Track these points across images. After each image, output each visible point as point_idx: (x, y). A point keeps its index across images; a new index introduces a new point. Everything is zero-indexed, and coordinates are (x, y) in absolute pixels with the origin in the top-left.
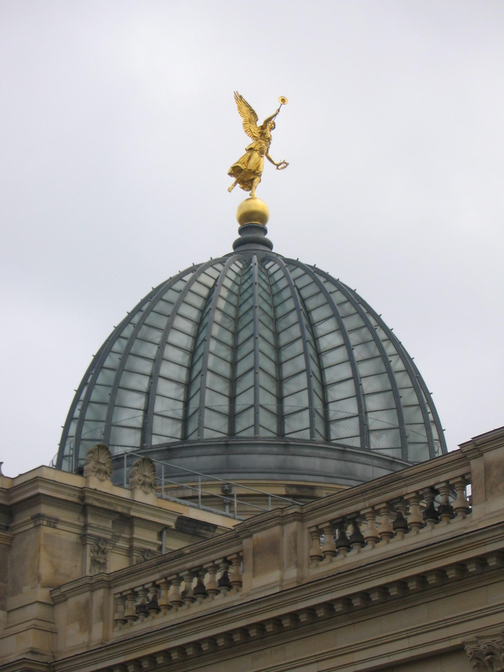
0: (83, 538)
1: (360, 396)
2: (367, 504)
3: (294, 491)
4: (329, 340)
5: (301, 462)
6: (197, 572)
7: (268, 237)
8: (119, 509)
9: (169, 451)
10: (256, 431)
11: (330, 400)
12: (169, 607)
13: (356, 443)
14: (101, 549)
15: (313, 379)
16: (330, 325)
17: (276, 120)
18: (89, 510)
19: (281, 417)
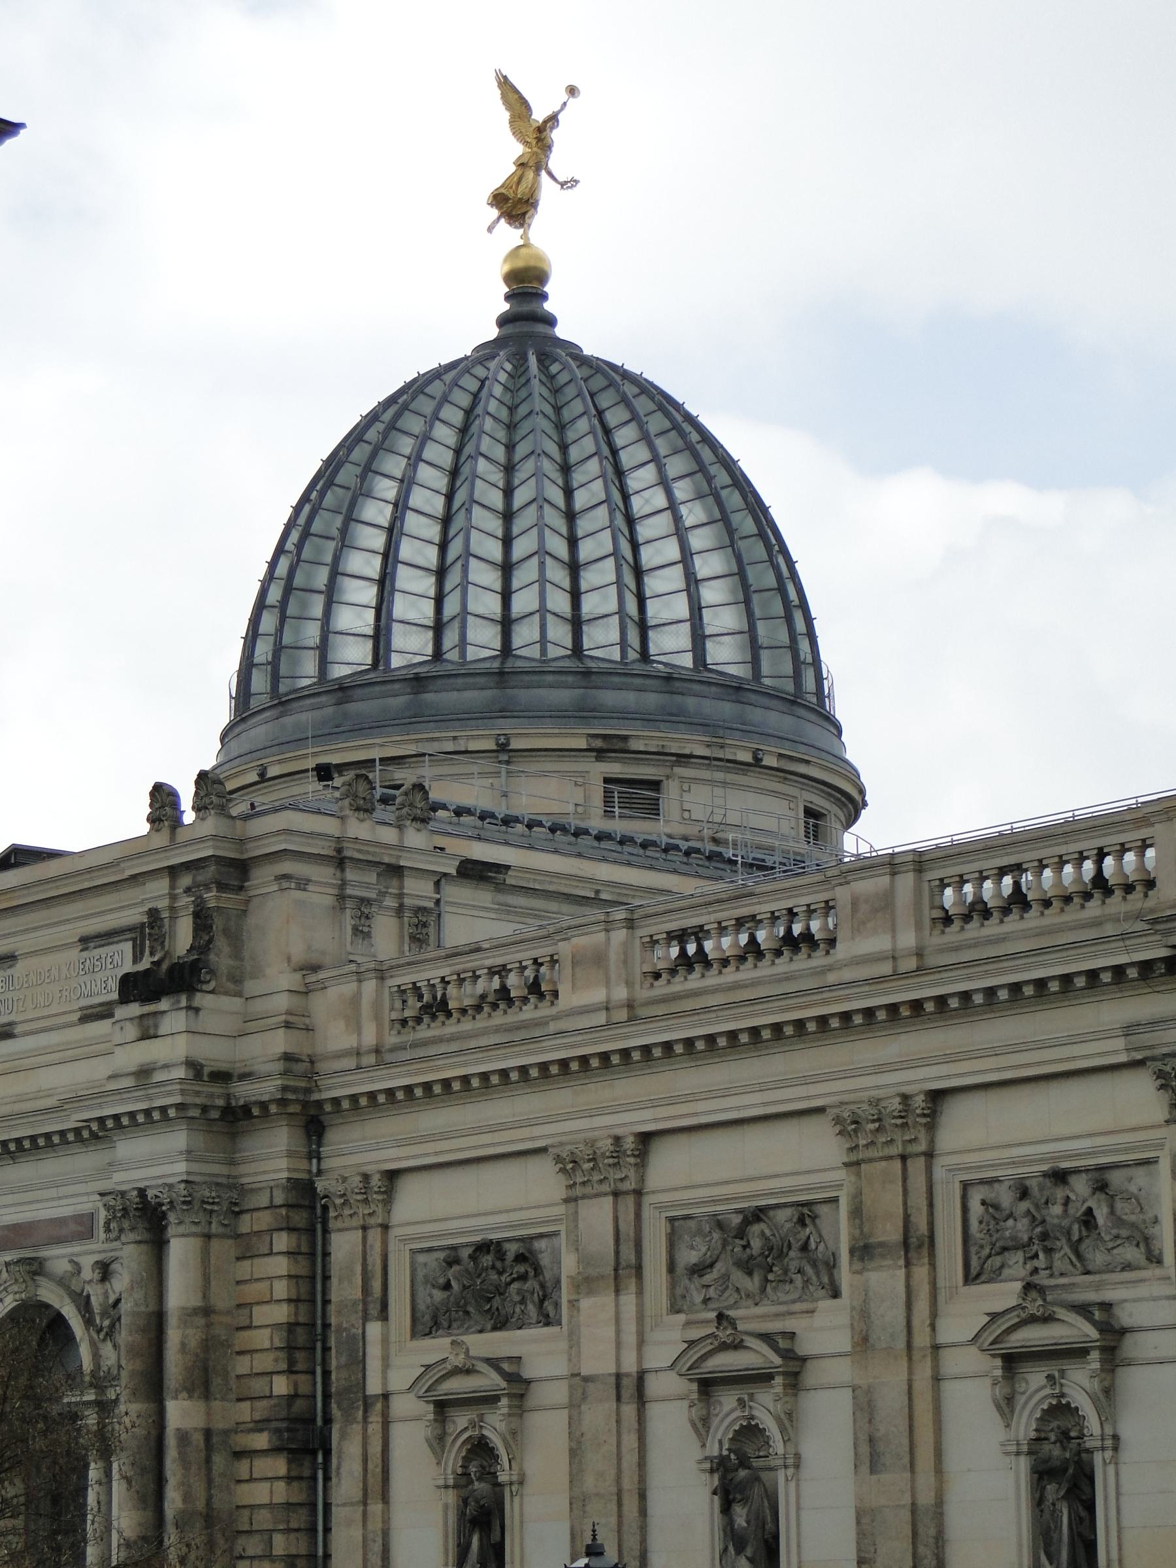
0: (342, 897)
1: (692, 583)
2: (713, 917)
3: (598, 743)
4: (648, 500)
5: (609, 698)
6: (501, 971)
7: (548, 306)
8: (386, 860)
9: (417, 681)
10: (544, 651)
11: (648, 594)
13: (687, 661)
15: (625, 567)
16: (648, 474)
17: (560, 117)
18: (348, 864)
19: (577, 623)
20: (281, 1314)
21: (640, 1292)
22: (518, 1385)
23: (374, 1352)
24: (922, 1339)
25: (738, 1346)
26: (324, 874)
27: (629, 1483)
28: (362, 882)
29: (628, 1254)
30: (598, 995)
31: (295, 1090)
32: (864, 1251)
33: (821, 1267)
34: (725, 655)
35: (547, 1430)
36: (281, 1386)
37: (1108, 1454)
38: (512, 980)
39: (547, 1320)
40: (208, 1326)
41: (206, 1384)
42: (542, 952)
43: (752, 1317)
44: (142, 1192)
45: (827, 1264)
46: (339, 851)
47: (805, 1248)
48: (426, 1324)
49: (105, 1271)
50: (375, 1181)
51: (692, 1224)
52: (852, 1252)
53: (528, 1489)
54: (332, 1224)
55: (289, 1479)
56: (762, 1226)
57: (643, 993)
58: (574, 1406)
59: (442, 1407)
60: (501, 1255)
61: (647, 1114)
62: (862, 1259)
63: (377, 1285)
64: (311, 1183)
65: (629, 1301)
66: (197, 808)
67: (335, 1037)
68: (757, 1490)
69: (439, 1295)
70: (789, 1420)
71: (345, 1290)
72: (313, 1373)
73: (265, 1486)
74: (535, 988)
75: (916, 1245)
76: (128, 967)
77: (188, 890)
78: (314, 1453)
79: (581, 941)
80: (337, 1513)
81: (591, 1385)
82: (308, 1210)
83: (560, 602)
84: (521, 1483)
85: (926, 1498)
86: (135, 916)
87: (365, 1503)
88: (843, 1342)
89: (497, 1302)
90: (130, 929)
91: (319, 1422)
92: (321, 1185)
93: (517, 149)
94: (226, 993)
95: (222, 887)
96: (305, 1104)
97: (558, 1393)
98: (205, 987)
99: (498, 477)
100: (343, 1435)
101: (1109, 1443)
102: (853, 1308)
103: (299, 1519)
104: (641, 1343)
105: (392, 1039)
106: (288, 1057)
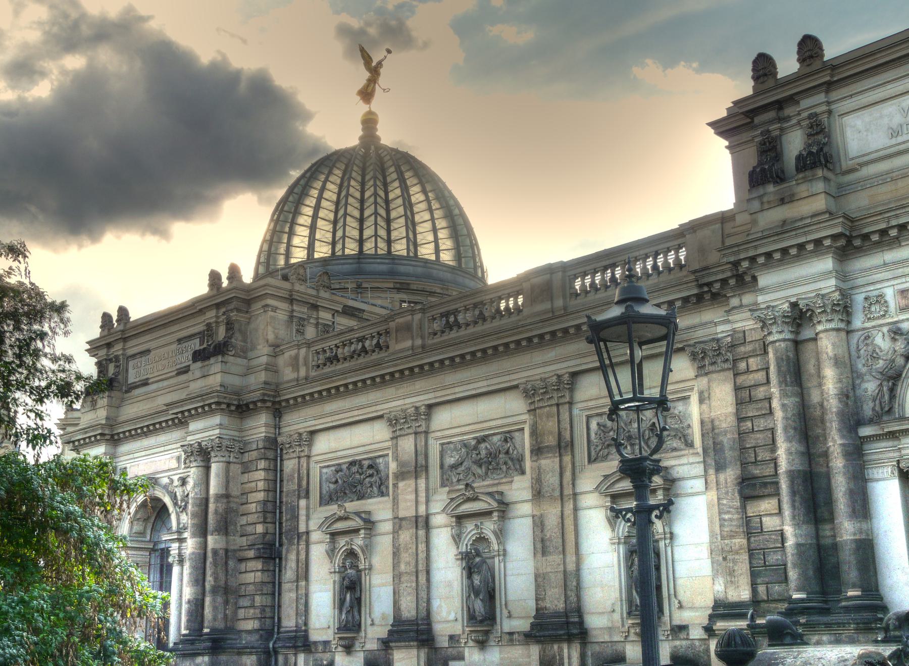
0: (291, 317)
1: (435, 230)
3: (398, 286)
6: (361, 339)
10: (376, 251)
12: (345, 359)
13: (433, 258)
14: (301, 324)
18: (295, 302)
19: (389, 242)
20: (261, 496)
21: (427, 478)
22: (370, 524)
23: (303, 512)
24: (568, 491)
25: (475, 499)
26: (284, 306)
27: (421, 567)
28: (301, 311)
29: (421, 460)
30: (408, 343)
31: (269, 396)
32: (538, 451)
33: (516, 462)
34: (447, 257)
35: (384, 544)
36: (260, 529)
37: (668, 541)
38: (367, 344)
39: (382, 494)
40: (228, 502)
41: (226, 529)
42: (381, 328)
43: (479, 485)
44: (200, 444)
45: (518, 460)
46: (291, 296)
47: (507, 453)
48: (327, 499)
49: (184, 482)
50: (304, 436)
51: (452, 446)
52: (532, 452)
53: (374, 572)
54: (285, 457)
55: (263, 571)
56: (487, 444)
57: (430, 342)
58: (395, 532)
59: (334, 535)
60: (361, 466)
61: (431, 395)
62: (537, 455)
63: (304, 483)
64: (275, 440)
65: (422, 483)
66: (229, 278)
67: (288, 374)
68: (484, 567)
69: (332, 486)
70: (501, 534)
71: (290, 486)
72: (275, 523)
73: (252, 574)
74: (378, 345)
75: (564, 446)
76: (198, 348)
77: (224, 314)
78: (274, 559)
79: (400, 320)
80: (286, 586)
81: (404, 523)
82: (274, 449)
83: (382, 233)
84: (370, 569)
85: (571, 567)
86: (201, 328)
87: (297, 581)
88: (527, 495)
89: (359, 487)
90: (199, 333)
91: (277, 545)
92: (280, 439)
93: (367, 75)
94: (239, 357)
95: (238, 310)
96: (274, 403)
97: (387, 527)
98: (230, 353)
99: (358, 205)
100: (288, 551)
101: (668, 536)
102: (532, 478)
103: (268, 589)
104: (427, 502)
105: (313, 373)
106: (265, 383)
